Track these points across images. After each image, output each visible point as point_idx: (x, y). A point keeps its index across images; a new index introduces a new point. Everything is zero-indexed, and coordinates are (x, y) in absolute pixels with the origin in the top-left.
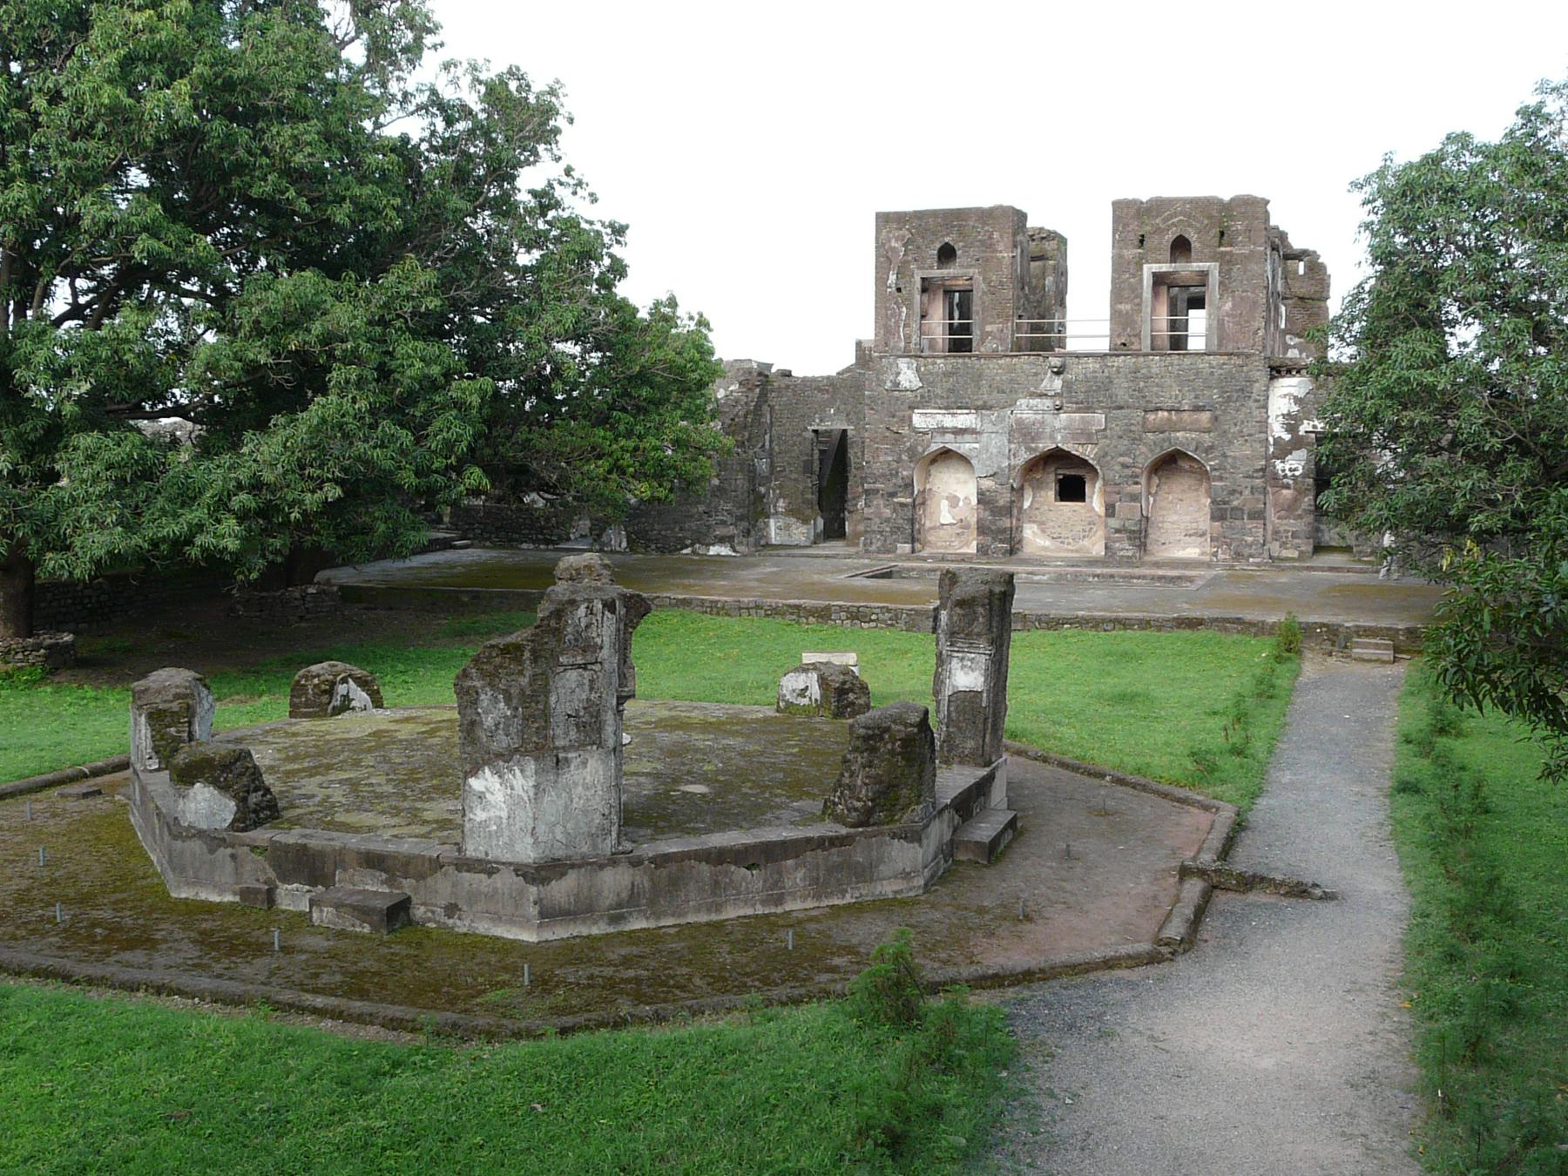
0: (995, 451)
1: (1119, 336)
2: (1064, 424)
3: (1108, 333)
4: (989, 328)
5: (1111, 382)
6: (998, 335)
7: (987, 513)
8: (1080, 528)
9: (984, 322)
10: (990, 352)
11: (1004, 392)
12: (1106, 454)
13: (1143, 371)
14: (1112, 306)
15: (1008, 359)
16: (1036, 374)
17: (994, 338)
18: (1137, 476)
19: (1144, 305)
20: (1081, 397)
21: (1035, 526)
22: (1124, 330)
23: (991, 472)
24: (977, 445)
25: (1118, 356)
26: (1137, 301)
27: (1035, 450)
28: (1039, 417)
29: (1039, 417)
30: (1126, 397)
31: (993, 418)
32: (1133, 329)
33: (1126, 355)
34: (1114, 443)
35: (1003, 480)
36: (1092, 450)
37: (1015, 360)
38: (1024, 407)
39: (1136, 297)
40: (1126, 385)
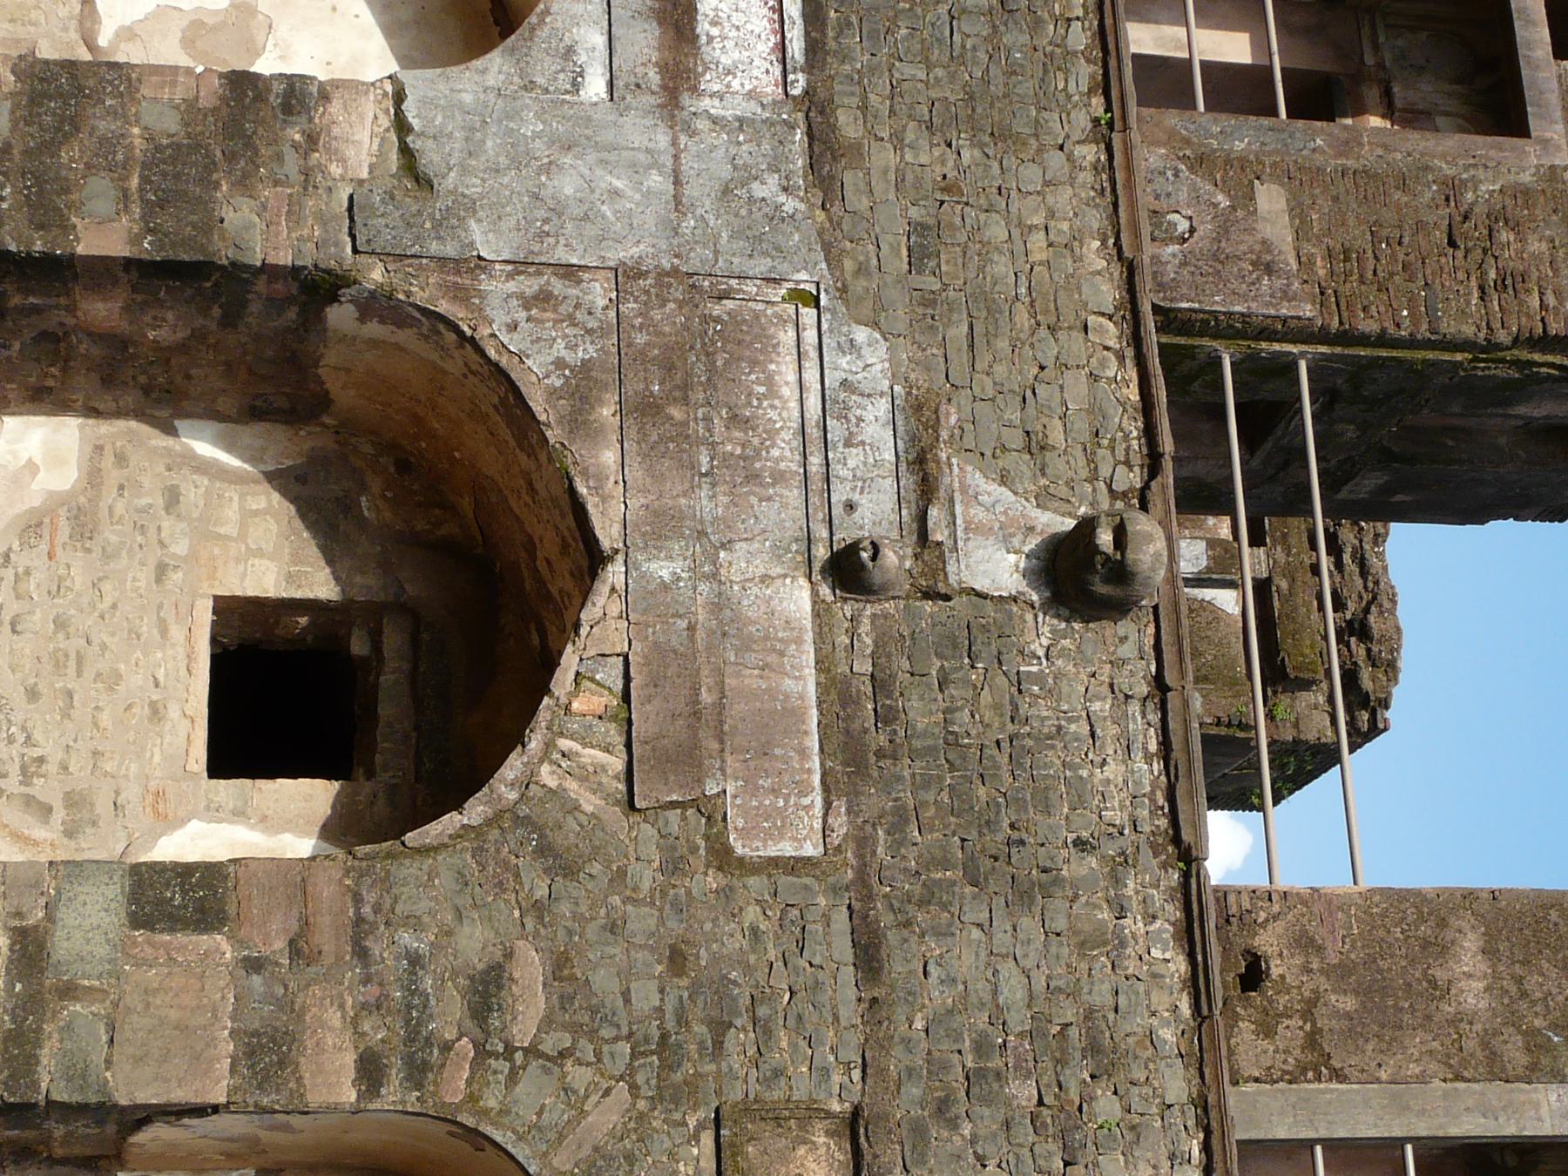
0: (567, 186)
1: (1304, 943)
2: (751, 603)
3: (1283, 882)
4: (1270, 199)
5: (1023, 895)
6: (1241, 244)
7: (170, 123)
8: (48, 746)
9: (1298, 178)
10: (1146, 200)
11: (918, 258)
12: (563, 866)
13: (1106, 1106)
14: (1469, 896)
15: (1108, 293)
16: (1035, 446)
17: (1224, 228)
18: (417, 1073)
19: (1495, 1091)
20: (921, 712)
21: (64, 478)
22: (1341, 973)
23: (430, 156)
24: (595, 87)
25: (1189, 935)
26: (1514, 1053)
27: (579, 421)
28: (784, 451)
29: (784, 451)
30: (938, 996)
31: (768, 188)
32: (1354, 1030)
33: (1197, 983)
34: (641, 921)
35: (383, 227)
36: (586, 776)
37: (1111, 333)
38: (841, 365)
39: (1536, 1044)
40: (1012, 990)
